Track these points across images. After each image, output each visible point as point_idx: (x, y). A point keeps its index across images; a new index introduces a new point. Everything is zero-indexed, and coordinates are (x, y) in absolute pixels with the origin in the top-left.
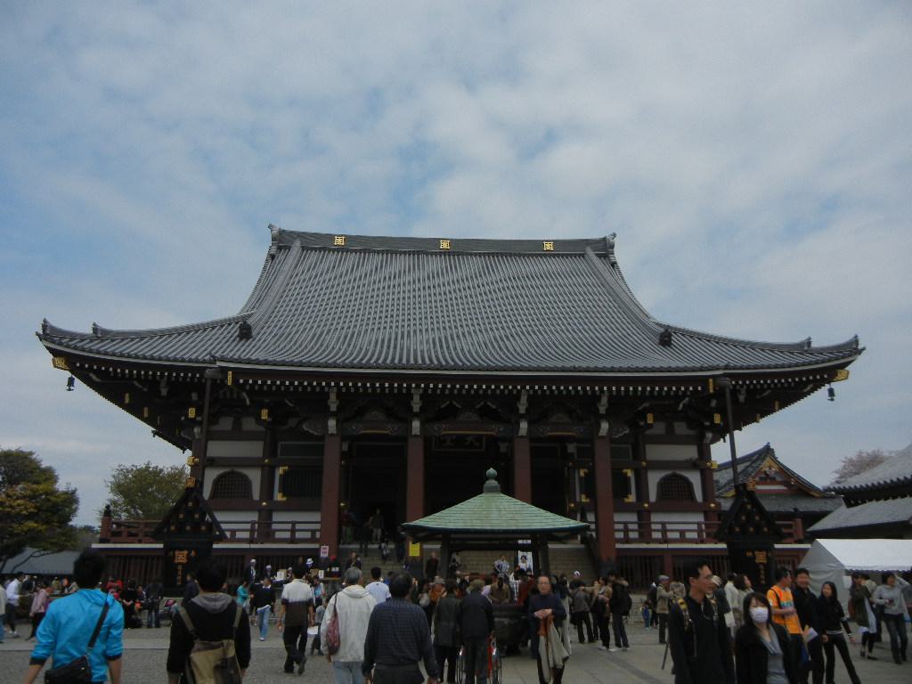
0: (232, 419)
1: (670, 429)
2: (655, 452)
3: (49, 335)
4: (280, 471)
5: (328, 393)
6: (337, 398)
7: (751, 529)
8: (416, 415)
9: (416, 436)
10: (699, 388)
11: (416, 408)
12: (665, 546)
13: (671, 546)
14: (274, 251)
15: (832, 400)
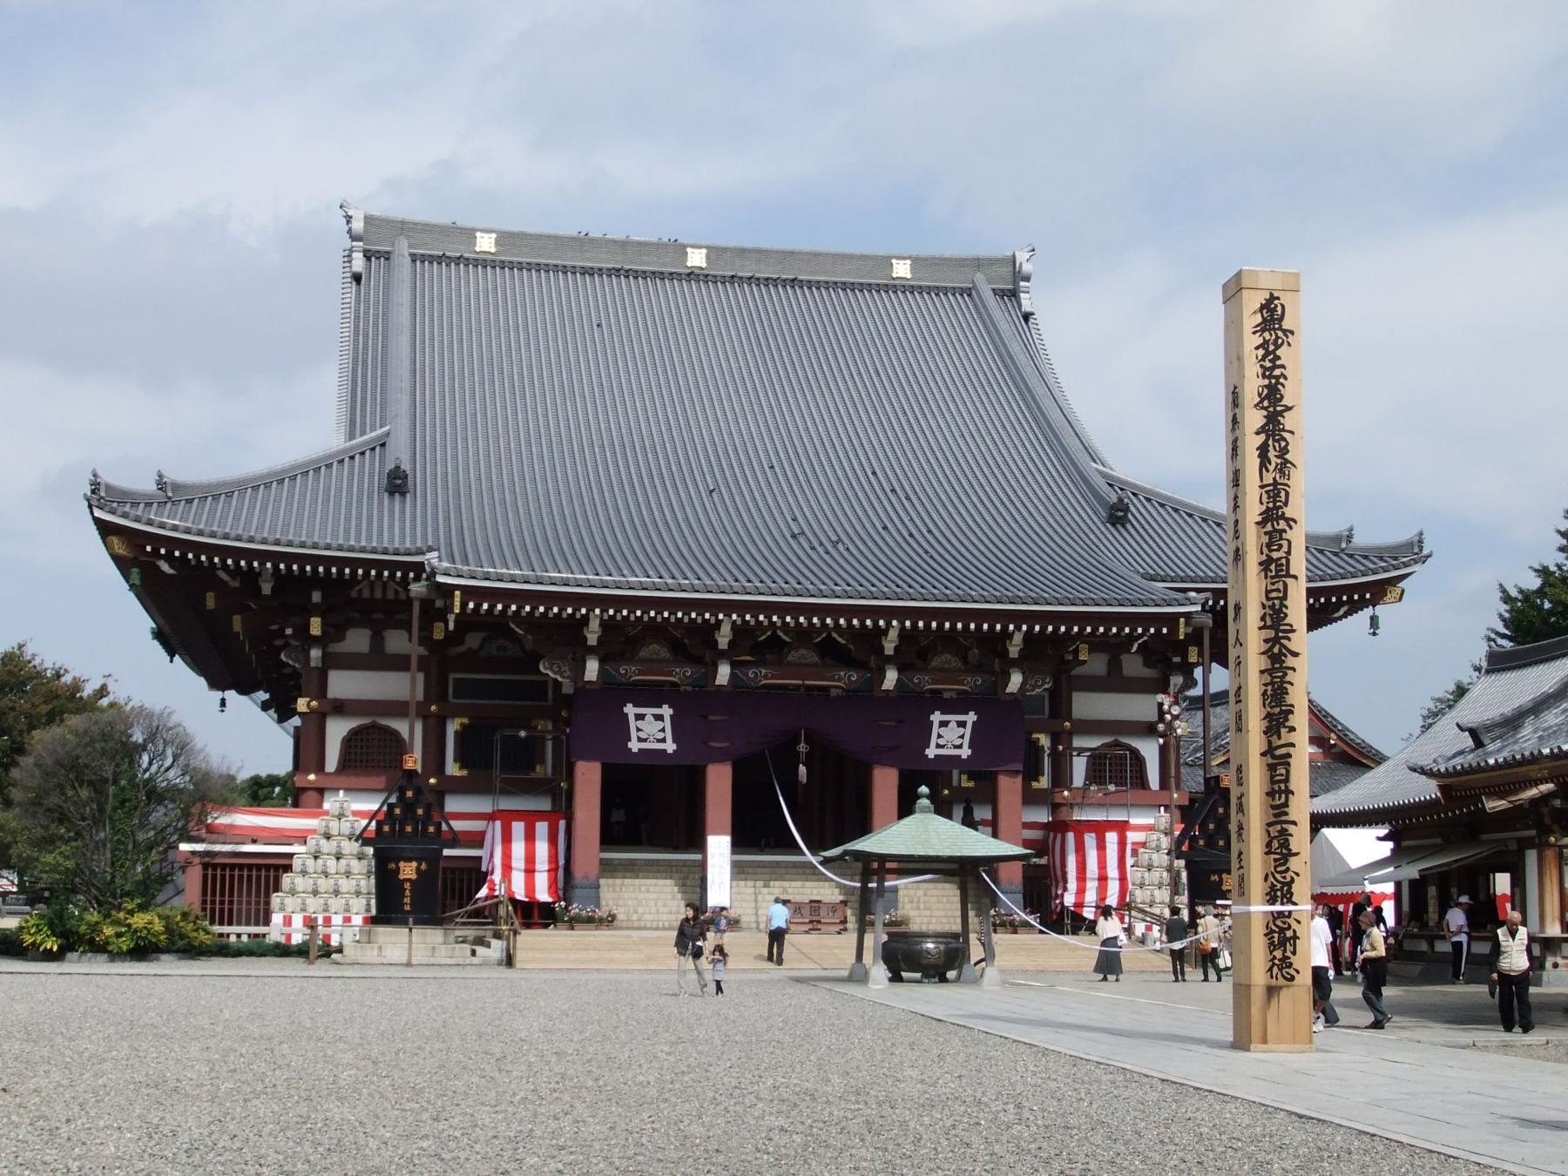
2: (1086, 705)
3: (99, 494)
4: (452, 727)
10: (1165, 631)
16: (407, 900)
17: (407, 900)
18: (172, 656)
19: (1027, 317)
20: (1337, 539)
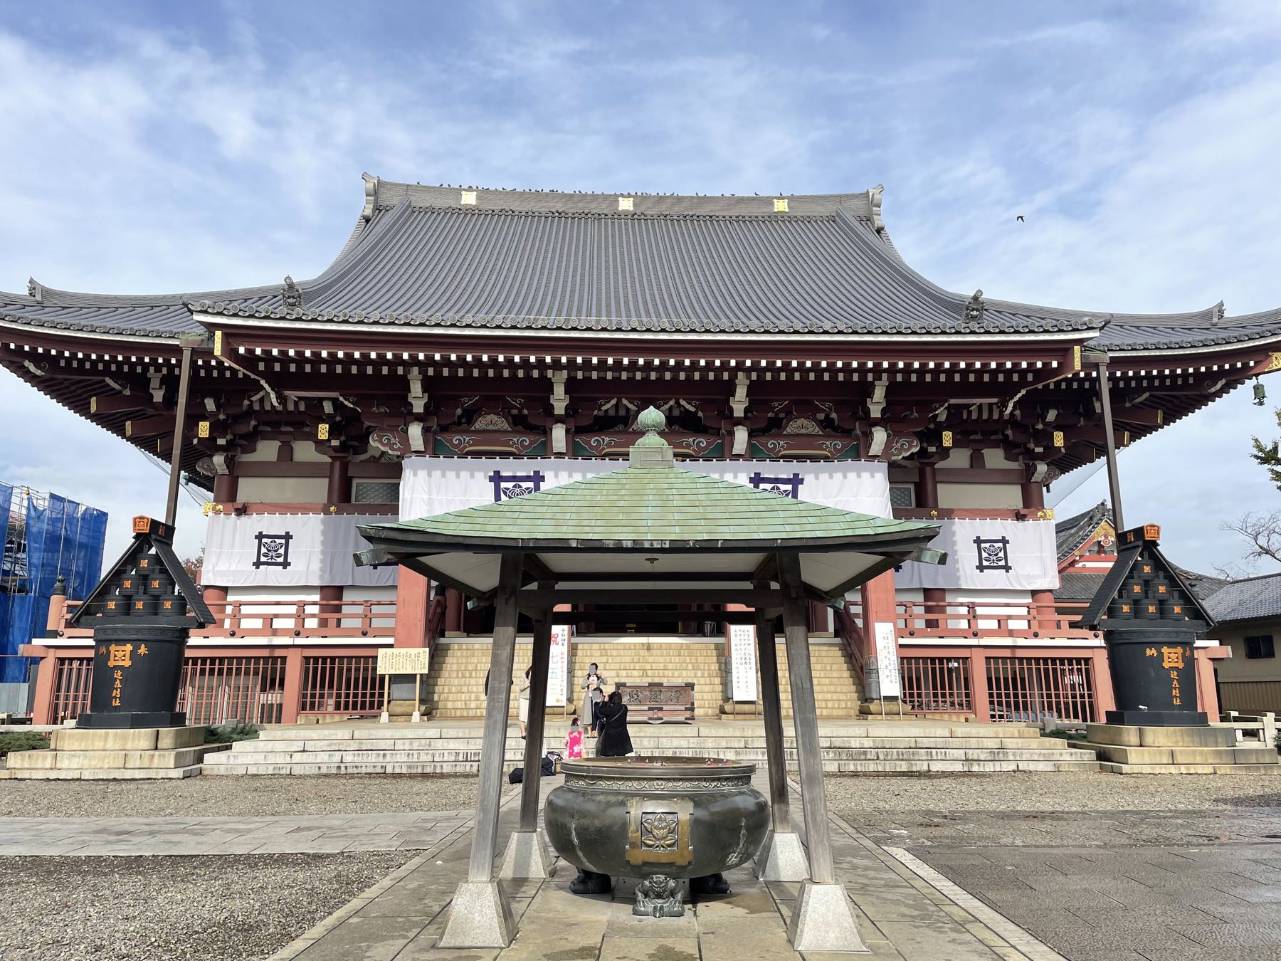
0: (277, 444)
1: (977, 460)
6: (424, 390)
7: (1152, 609)
8: (560, 420)
11: (560, 407)
14: (368, 212)
15: (1261, 403)
16: (117, 693)
17: (117, 693)
19: (879, 231)
20: (1207, 315)
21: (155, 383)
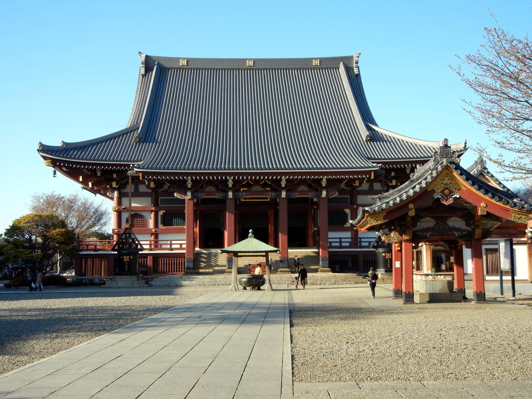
2: (361, 199)
4: (161, 213)
5: (187, 181)
8: (230, 189)
9: (231, 199)
12: (360, 250)
13: (362, 250)
18: (96, 194)
21: (98, 170)
